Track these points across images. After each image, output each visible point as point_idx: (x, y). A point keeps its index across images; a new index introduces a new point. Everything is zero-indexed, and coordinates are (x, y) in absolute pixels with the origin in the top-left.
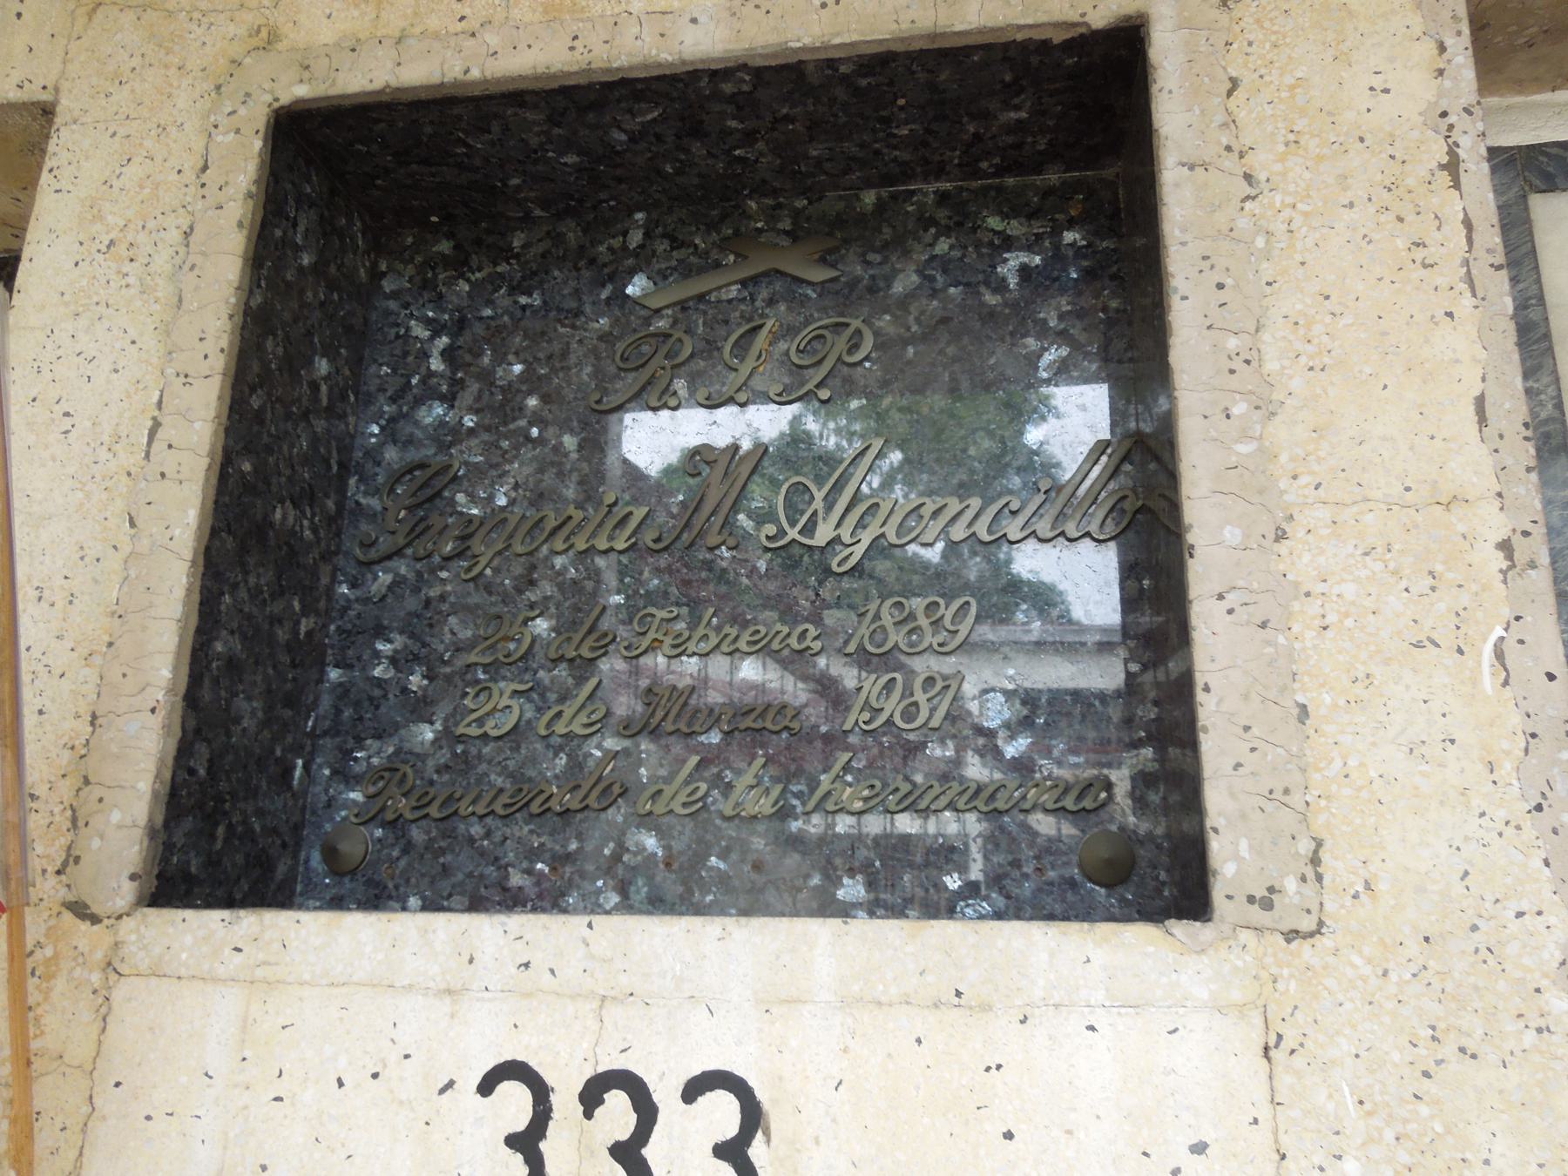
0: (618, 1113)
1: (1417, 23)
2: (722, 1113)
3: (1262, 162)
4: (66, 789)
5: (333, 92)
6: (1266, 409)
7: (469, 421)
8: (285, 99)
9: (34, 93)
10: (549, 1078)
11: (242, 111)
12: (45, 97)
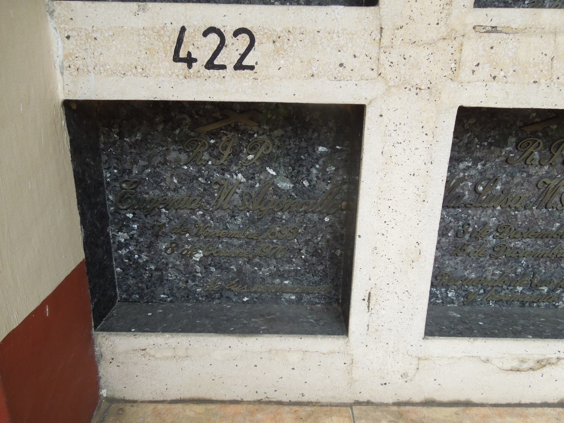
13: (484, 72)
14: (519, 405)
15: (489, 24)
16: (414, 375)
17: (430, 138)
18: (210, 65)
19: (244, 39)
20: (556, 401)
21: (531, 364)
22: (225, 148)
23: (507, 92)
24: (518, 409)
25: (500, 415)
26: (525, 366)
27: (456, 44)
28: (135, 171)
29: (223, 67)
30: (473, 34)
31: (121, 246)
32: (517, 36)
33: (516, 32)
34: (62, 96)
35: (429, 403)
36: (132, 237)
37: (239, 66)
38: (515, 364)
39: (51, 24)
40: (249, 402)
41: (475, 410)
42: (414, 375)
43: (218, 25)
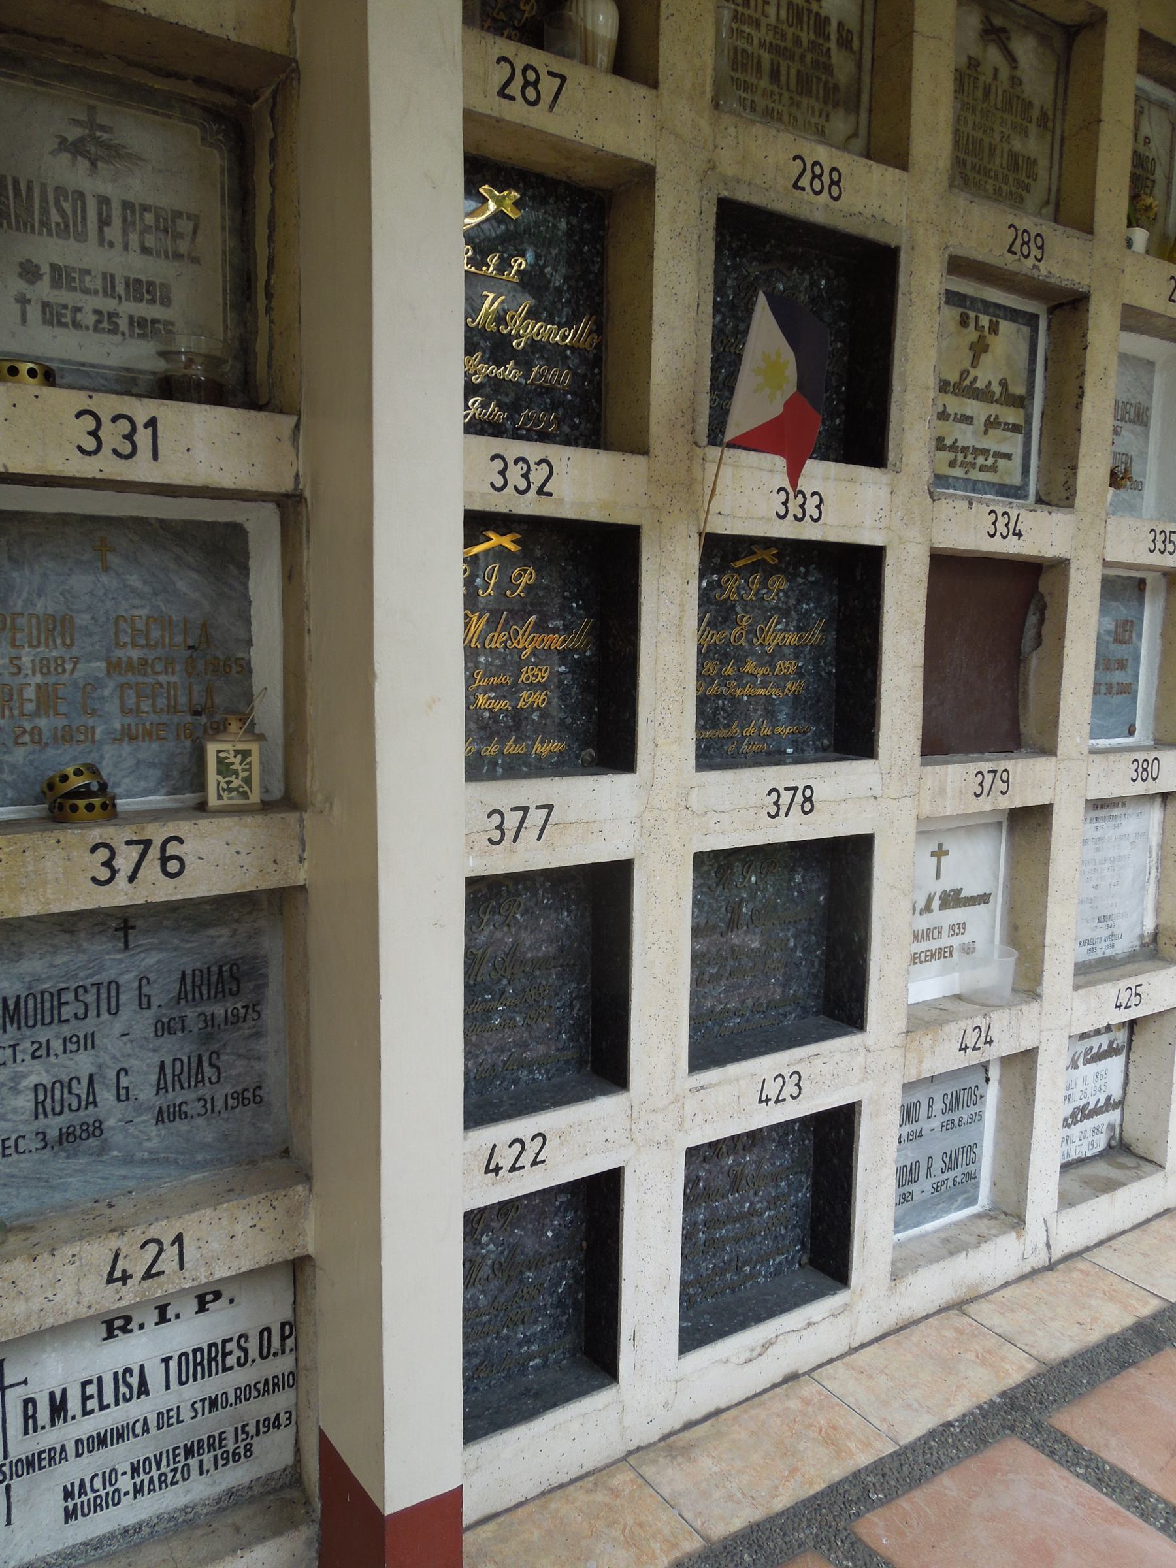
5: (735, 198)
8: (721, 196)
11: (710, 194)
12: (652, 163)
13: (699, 1119)
14: (756, 1395)
15: (698, 1085)
17: (669, 1178)
21: (758, 1350)
23: (715, 1130)
24: (756, 1399)
25: (746, 1411)
26: (755, 1354)
27: (680, 1104)
33: (715, 1085)
35: (688, 1426)
38: (747, 1355)
40: (534, 1499)
41: (724, 1416)
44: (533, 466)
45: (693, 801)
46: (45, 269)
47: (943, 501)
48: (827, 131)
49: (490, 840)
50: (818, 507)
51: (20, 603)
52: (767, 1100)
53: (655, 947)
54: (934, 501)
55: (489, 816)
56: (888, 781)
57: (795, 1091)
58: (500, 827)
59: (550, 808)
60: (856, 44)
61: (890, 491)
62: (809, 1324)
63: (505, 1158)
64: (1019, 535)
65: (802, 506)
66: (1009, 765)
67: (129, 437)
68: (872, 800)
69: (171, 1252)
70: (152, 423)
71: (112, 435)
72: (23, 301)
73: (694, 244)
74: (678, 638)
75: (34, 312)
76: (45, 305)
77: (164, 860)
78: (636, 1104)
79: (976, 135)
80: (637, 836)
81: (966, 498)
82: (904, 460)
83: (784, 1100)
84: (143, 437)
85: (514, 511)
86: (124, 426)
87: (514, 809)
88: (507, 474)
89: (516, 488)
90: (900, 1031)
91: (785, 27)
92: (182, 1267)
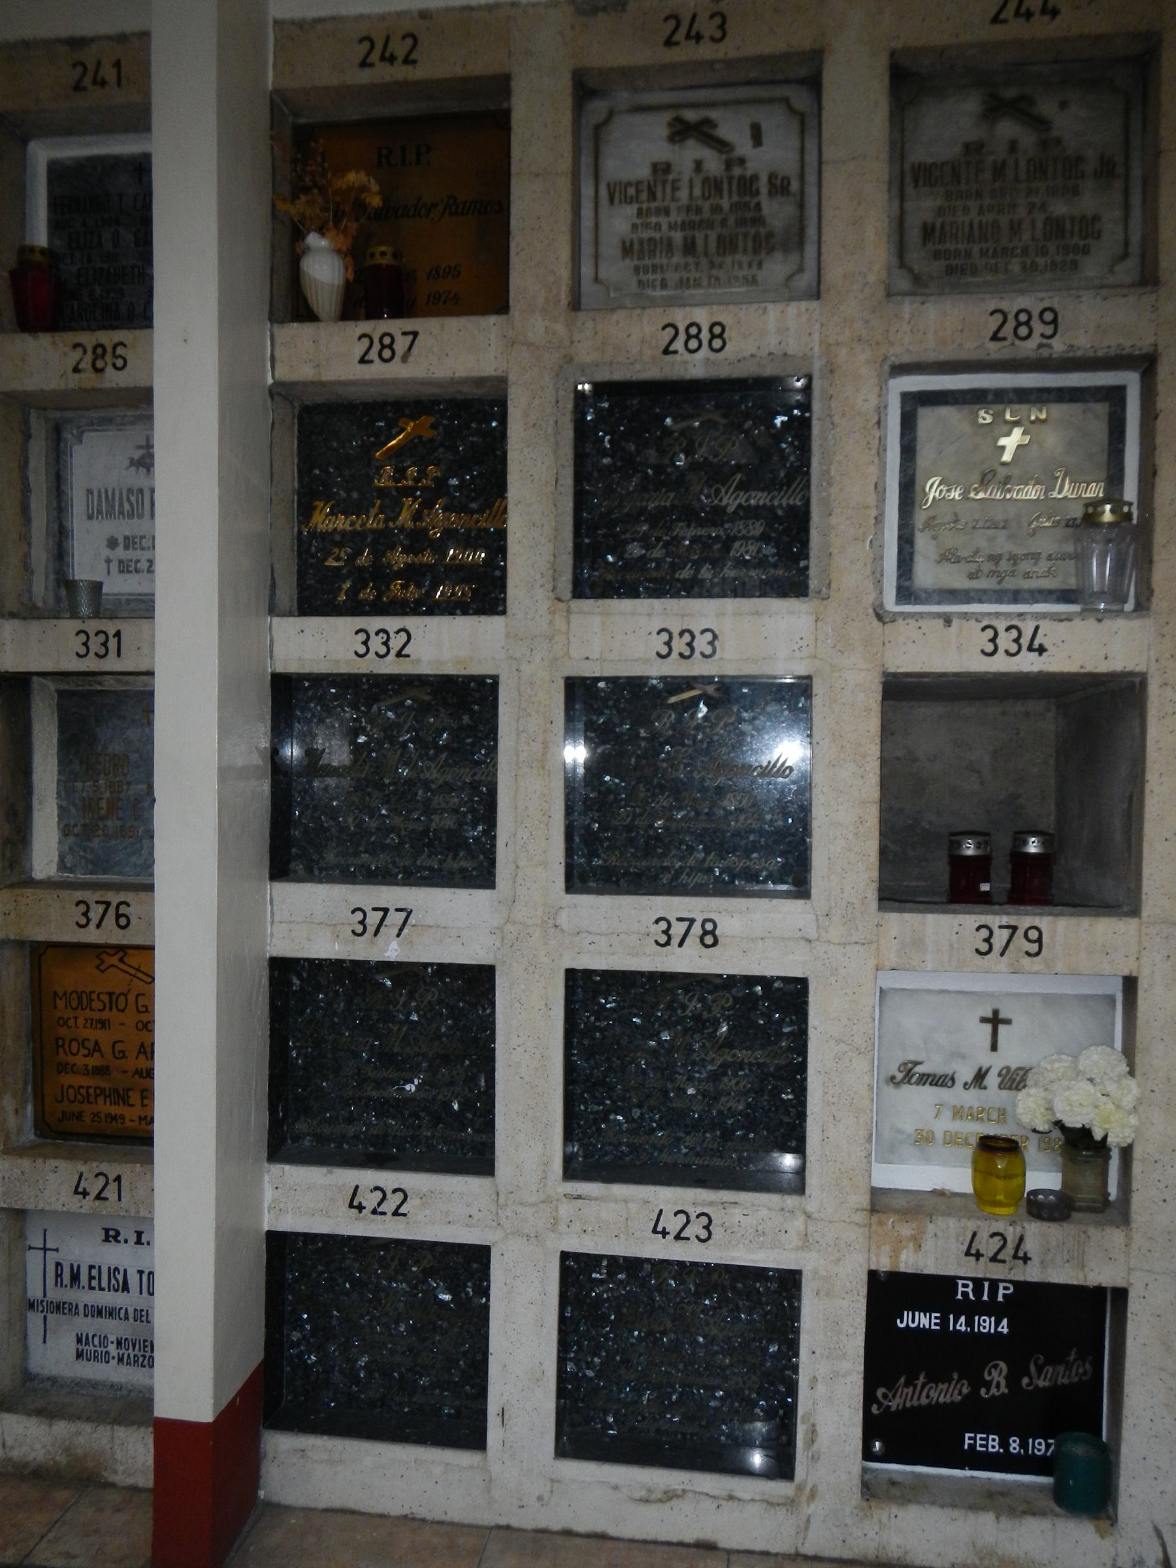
0: (687, 638)
1: (876, 380)
2: (709, 636)
3: (836, 419)
4: (551, 572)
6: (830, 484)
7: (619, 464)
9: (499, 373)
10: (672, 631)
11: (566, 384)
12: (504, 374)
13: (577, 1227)
15: (575, 1193)
16: (549, 1499)
18: (374, 1212)
19: (400, 1196)
20: (692, 1541)
21: (659, 1495)
22: (393, 1259)
23: (596, 1243)
26: (653, 1497)
28: (314, 1275)
29: (384, 1214)
30: (564, 1199)
31: (294, 1345)
32: (598, 1202)
33: (596, 1199)
34: (266, 1227)
36: (304, 1337)
37: (396, 1213)
38: (643, 1493)
39: (267, 1178)
41: (609, 1544)
42: (549, 1499)
43: (381, 1185)
44: (392, 635)
45: (563, 919)
46: (121, 540)
47: (900, 621)
48: (759, 278)
49: (353, 932)
50: (711, 643)
51: (100, 747)
52: (664, 1233)
53: (520, 1050)
54: (884, 623)
55: (353, 912)
56: (827, 923)
57: (704, 1234)
58: (362, 922)
59: (409, 913)
60: (795, 186)
61: (814, 618)
62: (731, 1498)
63: (370, 1200)
64: (1041, 650)
65: (690, 645)
66: (1044, 922)
67: (105, 644)
68: (802, 942)
69: (113, 1186)
70: (118, 634)
71: (95, 644)
72: (108, 561)
73: (550, 430)
74: (541, 772)
75: (114, 567)
76: (121, 562)
77: (118, 916)
78: (502, 1189)
79: (984, 219)
80: (498, 944)
81: (939, 615)
82: (833, 586)
83: (688, 1239)
84: (112, 644)
85: (375, 671)
86: (102, 637)
87: (375, 909)
88: (369, 643)
89: (377, 654)
90: (857, 1206)
91: (700, 202)
92: (120, 1199)
